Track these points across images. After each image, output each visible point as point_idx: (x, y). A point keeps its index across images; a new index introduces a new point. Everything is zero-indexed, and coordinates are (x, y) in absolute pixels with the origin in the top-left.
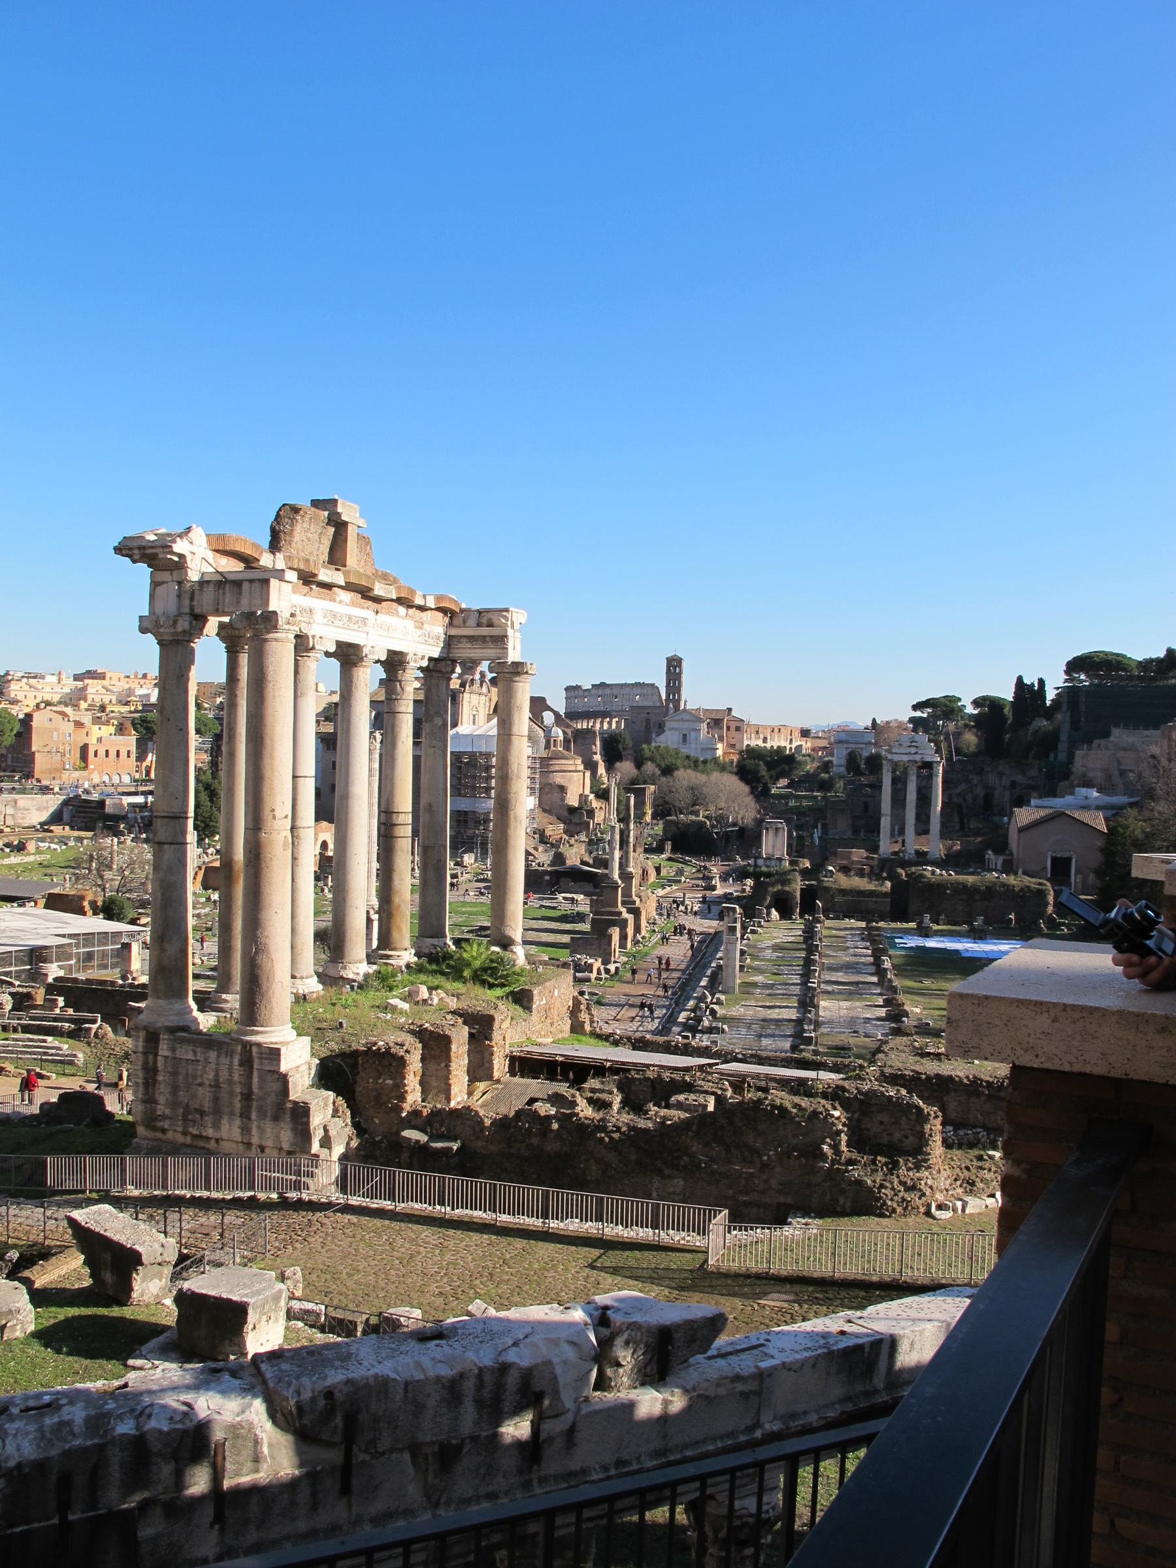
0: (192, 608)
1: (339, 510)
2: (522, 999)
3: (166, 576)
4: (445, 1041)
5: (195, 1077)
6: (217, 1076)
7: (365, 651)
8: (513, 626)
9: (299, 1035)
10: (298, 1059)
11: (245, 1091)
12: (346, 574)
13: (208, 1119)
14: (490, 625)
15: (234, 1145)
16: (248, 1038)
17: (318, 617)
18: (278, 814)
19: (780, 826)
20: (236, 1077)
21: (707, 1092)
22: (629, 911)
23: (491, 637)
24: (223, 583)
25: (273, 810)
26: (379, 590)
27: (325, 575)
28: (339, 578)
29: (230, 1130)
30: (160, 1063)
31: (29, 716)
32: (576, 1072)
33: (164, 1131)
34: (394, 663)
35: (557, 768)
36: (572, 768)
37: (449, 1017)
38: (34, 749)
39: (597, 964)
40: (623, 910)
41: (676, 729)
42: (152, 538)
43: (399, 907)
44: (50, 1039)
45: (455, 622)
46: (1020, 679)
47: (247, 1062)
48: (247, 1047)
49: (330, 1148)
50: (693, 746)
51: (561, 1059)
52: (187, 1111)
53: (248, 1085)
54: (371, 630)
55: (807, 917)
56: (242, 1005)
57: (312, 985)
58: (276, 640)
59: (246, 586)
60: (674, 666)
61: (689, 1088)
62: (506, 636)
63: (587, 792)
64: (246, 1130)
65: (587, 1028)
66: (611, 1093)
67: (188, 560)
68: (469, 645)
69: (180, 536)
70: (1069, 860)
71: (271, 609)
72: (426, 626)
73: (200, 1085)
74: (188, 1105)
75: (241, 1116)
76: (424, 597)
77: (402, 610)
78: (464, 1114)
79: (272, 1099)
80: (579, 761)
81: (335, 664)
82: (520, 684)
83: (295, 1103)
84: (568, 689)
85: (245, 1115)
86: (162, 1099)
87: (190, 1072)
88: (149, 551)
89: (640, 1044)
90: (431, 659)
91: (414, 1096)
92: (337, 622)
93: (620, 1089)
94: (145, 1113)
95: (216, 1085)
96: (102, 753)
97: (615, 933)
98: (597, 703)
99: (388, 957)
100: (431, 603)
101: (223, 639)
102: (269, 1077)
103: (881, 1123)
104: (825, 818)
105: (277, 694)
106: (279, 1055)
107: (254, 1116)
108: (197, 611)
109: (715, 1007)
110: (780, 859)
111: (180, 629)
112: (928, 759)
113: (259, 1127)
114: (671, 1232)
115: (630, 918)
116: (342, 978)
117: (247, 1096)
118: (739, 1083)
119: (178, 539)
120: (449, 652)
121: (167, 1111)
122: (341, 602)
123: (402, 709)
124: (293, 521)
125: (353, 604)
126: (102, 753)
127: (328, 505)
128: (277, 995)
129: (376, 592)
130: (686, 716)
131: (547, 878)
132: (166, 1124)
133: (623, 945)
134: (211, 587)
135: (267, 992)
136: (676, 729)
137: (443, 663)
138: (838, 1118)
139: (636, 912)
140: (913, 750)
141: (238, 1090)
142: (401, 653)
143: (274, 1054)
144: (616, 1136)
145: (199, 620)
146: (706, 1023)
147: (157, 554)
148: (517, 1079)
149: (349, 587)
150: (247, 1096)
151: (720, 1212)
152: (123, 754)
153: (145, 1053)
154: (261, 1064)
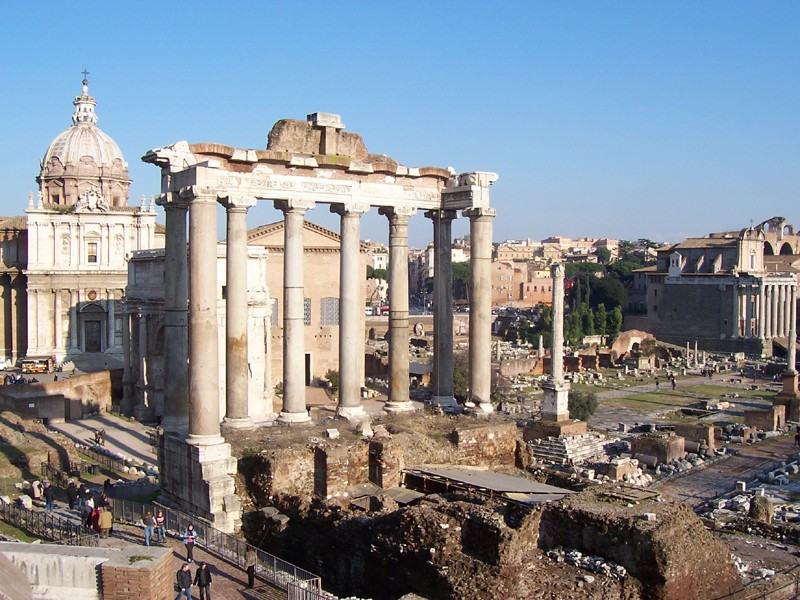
28: (313, 162)
43: (397, 373)
47: (189, 456)
53: (190, 468)
64: (190, 495)
65: (525, 463)
77: (389, 179)
82: (481, 223)
85: (190, 487)
86: (166, 474)
96: (532, 289)
100: (415, 172)
117: (190, 474)
122: (323, 177)
125: (333, 178)
126: (532, 289)
127: (313, 117)
128: (203, 415)
129: (351, 169)
152: (546, 289)
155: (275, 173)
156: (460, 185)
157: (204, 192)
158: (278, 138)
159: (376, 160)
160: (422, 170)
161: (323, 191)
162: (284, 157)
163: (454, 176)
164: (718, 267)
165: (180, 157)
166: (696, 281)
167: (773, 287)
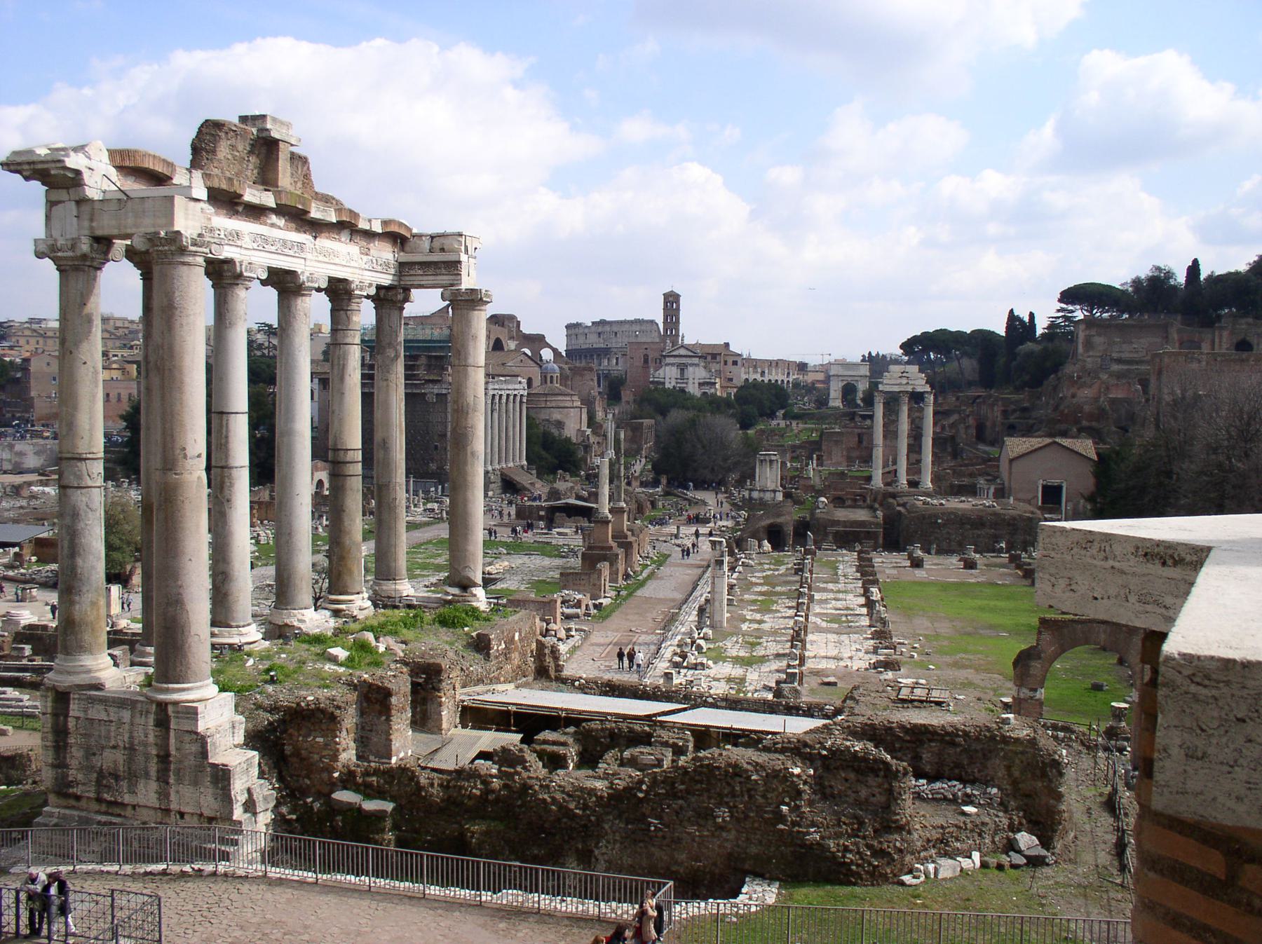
0: (91, 228)
1: (269, 126)
2: (481, 645)
3: (62, 195)
4: (388, 693)
5: (108, 738)
6: (131, 737)
7: (303, 278)
8: (466, 251)
9: (223, 690)
10: (219, 718)
11: (162, 753)
12: (277, 194)
13: (124, 784)
14: (442, 250)
15: (152, 812)
16: (162, 697)
17: (247, 241)
18: (191, 451)
19: (773, 458)
20: (151, 739)
21: (666, 744)
22: (620, 545)
23: (444, 262)
24: (124, 199)
25: (184, 449)
26: (315, 213)
27: (252, 195)
28: (269, 200)
29: (147, 793)
30: (71, 724)
31: (26, 360)
32: (529, 723)
33: (78, 798)
34: (339, 291)
37: (393, 666)
38: (33, 394)
39: (586, 600)
40: (614, 545)
41: (673, 364)
42: (42, 152)
44: (9, 690)
45: (407, 248)
46: (1012, 311)
47: (163, 723)
48: (162, 706)
49: (255, 814)
50: (691, 381)
51: (513, 708)
52: (101, 774)
54: (309, 256)
55: (798, 548)
56: (156, 659)
57: (251, 634)
58: (184, 264)
59: (148, 204)
60: (671, 302)
61: (645, 739)
62: (460, 262)
63: (584, 428)
64: (164, 795)
65: (552, 673)
66: (564, 744)
67: (86, 176)
68: (420, 272)
69: (76, 150)
70: (1059, 488)
71: (176, 229)
72: (372, 251)
73: (114, 747)
74: (101, 769)
75: (158, 780)
76: (370, 221)
77: (345, 236)
78: (404, 774)
79: (191, 761)
80: (575, 398)
81: (271, 294)
83: (215, 766)
85: (163, 778)
86: (74, 763)
87: (103, 734)
88: (40, 166)
89: (612, 690)
90: (379, 288)
91: (348, 754)
92: (268, 247)
93: (577, 740)
94: (56, 779)
95: (131, 749)
97: (605, 567)
98: (593, 341)
99: (339, 602)
100: (378, 228)
101: (137, 265)
102: (187, 738)
103: (846, 780)
104: (820, 449)
105: (184, 322)
106: (197, 714)
107: (171, 781)
108: (99, 233)
109: (702, 642)
110: (774, 491)
111: (79, 253)
112: (919, 389)
113: (177, 792)
114: (614, 904)
115: (621, 552)
116: (286, 625)
117: (164, 758)
118: (703, 736)
119: (72, 153)
120: (400, 280)
121: (80, 777)
123: (349, 340)
124: (215, 139)
128: (194, 650)
130: (682, 352)
131: (542, 513)
132: (77, 790)
133: (613, 579)
134: (114, 206)
135: (183, 645)
136: (673, 364)
137: (394, 292)
138: (799, 776)
139: (627, 546)
140: (904, 381)
141: (154, 752)
142: (345, 281)
143: (191, 713)
144: (559, 796)
145: (103, 243)
146: (692, 659)
147: (47, 170)
148: (468, 732)
149: (281, 210)
150: (164, 758)
151: (665, 884)
153: (55, 715)
154: (178, 724)
155: (217, 214)
157: (194, 244)
158: (214, 152)
159: (327, 200)
160: (385, 223)
161: (273, 249)
162: (236, 188)
163: (420, 236)
165: (100, 179)
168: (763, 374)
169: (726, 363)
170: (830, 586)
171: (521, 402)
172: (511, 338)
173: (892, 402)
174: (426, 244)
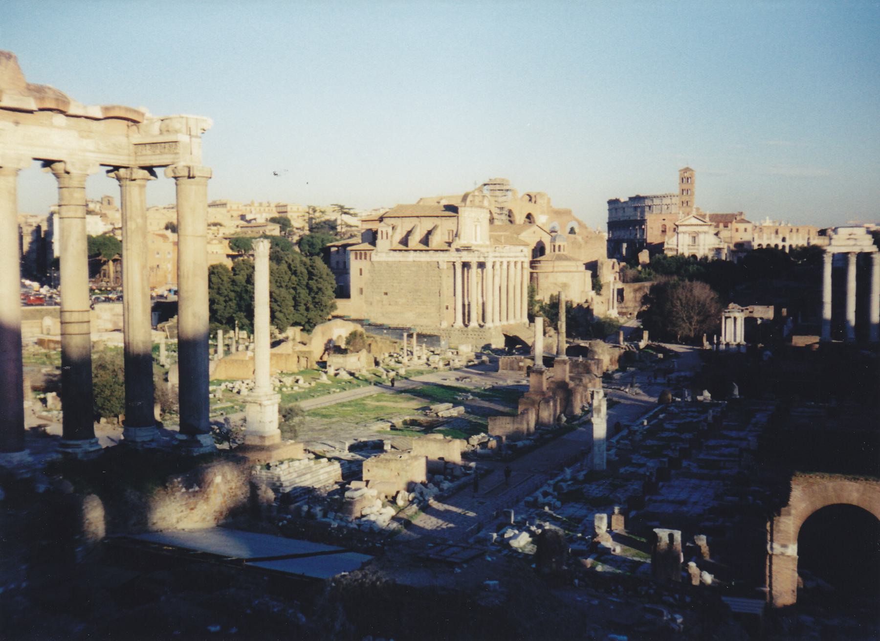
35: (561, 269)
36: (574, 269)
60: (686, 177)
84: (611, 202)
112: (867, 250)
140: (852, 242)
156: (161, 132)
160: (107, 109)
164: (437, 240)
166: (411, 257)
167: (502, 262)
168: (784, 240)
169: (737, 230)
170: (733, 434)
171: (522, 268)
172: (543, 213)
173: (841, 261)
174: (156, 128)
